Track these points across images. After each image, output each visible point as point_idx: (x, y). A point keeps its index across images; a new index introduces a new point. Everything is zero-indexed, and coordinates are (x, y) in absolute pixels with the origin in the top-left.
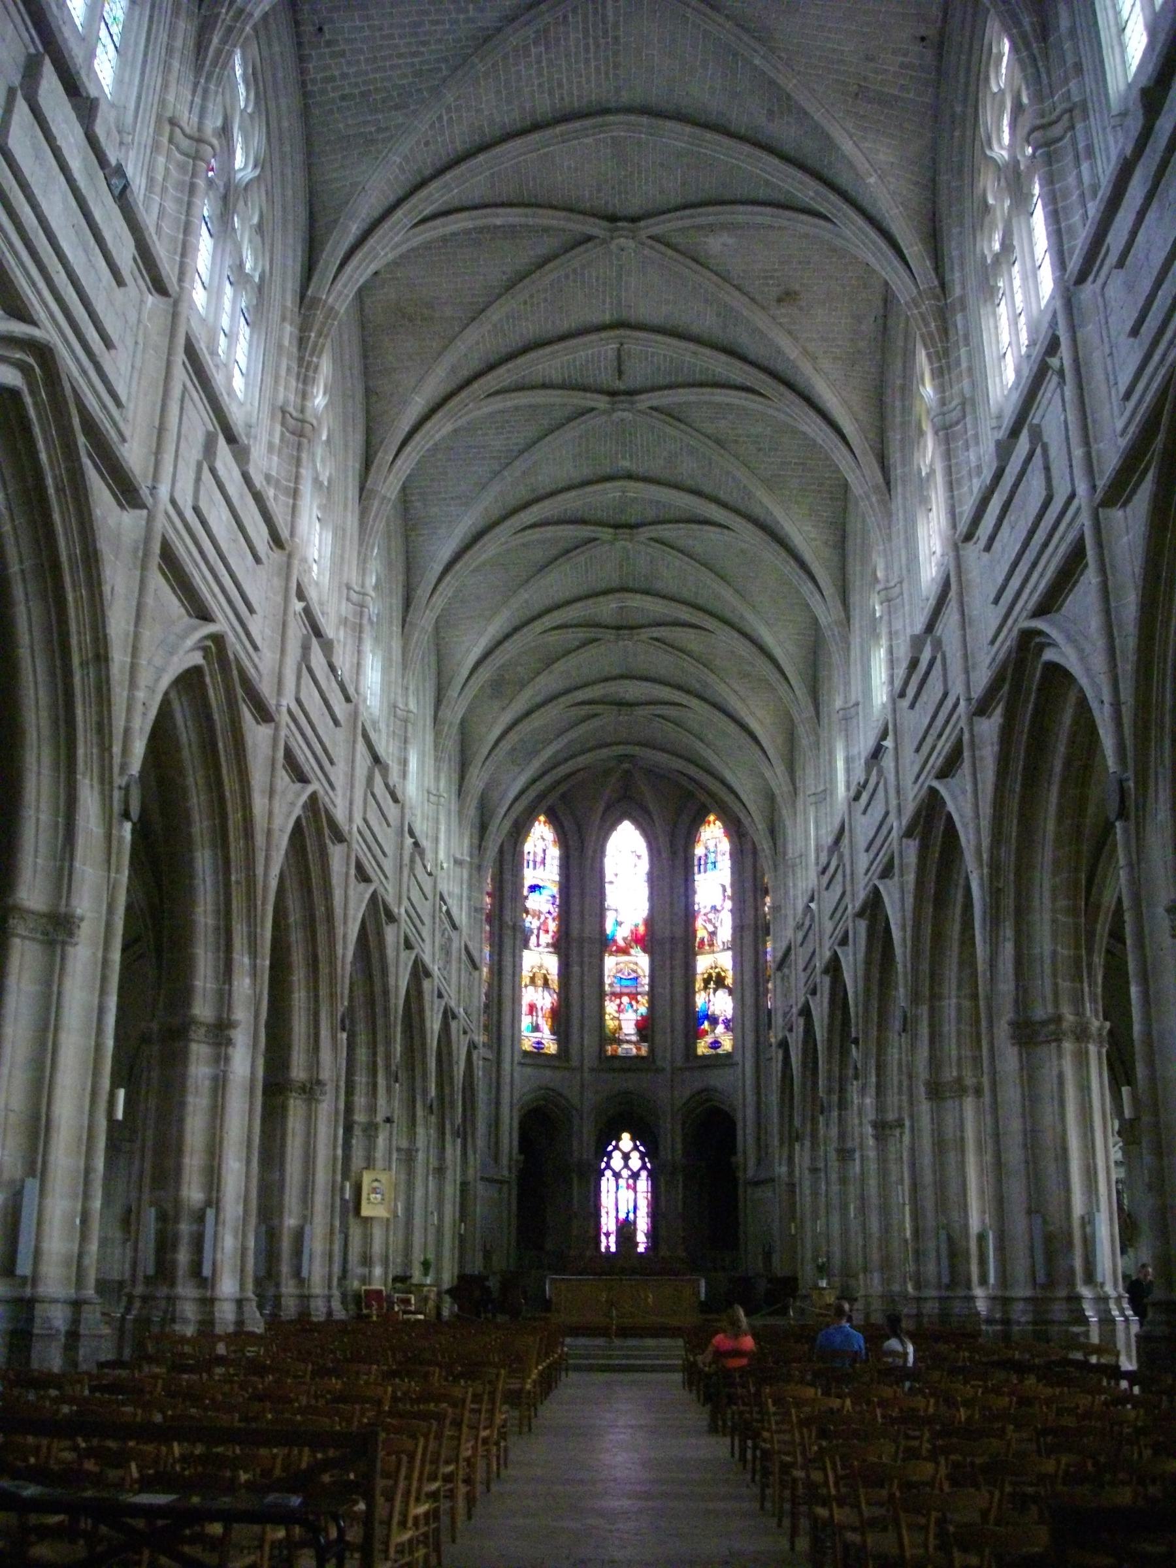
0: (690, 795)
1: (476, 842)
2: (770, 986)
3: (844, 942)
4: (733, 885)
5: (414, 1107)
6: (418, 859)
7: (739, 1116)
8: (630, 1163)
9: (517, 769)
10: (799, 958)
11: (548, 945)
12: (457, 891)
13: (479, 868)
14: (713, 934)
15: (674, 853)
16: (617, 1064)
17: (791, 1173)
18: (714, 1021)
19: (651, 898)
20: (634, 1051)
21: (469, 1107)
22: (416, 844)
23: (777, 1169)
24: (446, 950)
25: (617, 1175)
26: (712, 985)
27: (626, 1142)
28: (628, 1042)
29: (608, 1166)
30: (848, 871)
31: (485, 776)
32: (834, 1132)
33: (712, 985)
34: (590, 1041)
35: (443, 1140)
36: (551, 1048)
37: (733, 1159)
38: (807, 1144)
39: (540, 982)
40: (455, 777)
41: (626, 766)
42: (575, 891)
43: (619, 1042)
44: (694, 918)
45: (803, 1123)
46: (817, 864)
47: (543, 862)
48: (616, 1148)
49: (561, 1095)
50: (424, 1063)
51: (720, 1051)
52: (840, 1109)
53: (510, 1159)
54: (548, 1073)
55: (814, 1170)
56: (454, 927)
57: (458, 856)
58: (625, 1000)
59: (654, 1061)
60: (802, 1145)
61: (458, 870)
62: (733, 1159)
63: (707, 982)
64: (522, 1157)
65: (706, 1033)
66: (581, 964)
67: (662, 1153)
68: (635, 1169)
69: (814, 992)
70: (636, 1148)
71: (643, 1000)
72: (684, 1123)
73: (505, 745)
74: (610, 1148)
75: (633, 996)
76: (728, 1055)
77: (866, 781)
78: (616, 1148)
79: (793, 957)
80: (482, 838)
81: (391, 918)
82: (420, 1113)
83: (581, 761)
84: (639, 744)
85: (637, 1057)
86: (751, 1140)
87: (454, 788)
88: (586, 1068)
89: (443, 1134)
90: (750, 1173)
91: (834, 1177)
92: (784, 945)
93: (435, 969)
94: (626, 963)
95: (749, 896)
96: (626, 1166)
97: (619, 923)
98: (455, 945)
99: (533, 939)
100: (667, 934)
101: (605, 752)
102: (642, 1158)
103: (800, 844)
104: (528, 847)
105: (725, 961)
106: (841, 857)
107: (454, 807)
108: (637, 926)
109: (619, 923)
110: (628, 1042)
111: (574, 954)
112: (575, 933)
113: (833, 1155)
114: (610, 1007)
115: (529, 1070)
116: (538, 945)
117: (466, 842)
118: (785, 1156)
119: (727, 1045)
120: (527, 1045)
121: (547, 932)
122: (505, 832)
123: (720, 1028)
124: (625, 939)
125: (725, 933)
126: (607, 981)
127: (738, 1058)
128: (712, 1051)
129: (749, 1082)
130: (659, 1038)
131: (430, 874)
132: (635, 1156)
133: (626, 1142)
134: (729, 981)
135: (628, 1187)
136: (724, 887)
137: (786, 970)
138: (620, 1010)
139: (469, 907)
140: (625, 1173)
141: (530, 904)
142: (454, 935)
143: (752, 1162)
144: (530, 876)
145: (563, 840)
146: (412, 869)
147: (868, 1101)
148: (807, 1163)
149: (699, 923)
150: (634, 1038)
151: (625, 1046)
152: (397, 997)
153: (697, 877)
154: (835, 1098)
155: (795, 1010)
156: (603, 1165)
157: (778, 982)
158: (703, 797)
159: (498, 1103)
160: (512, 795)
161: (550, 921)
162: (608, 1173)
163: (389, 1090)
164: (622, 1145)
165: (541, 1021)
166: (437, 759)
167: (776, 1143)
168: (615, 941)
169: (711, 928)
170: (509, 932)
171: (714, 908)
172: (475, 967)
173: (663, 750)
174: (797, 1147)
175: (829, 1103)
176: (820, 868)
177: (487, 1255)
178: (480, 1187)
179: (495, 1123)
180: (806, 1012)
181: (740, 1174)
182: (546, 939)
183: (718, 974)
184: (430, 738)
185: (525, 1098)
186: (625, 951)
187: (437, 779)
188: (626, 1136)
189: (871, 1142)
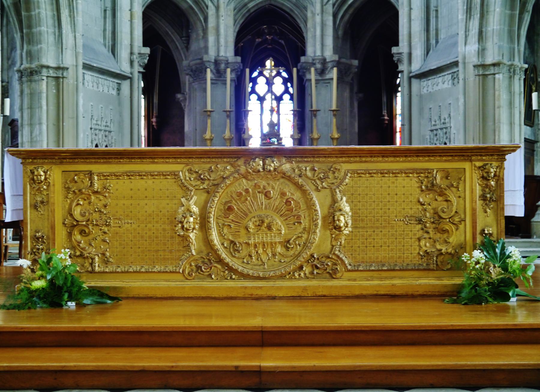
8: (274, 87)
17: (482, 52)
23: (461, 48)
25: (261, 99)
29: (253, 91)
53: (132, 53)
62: (394, 50)
64: (147, 50)
67: (310, 50)
68: (278, 94)
72: (335, 16)
74: (255, 74)
78: (261, 74)
86: (417, 26)
96: (270, 91)
132: (278, 81)
135: (272, 111)
140: (269, 97)
162: (254, 97)
164: (266, 73)
167: (461, 16)
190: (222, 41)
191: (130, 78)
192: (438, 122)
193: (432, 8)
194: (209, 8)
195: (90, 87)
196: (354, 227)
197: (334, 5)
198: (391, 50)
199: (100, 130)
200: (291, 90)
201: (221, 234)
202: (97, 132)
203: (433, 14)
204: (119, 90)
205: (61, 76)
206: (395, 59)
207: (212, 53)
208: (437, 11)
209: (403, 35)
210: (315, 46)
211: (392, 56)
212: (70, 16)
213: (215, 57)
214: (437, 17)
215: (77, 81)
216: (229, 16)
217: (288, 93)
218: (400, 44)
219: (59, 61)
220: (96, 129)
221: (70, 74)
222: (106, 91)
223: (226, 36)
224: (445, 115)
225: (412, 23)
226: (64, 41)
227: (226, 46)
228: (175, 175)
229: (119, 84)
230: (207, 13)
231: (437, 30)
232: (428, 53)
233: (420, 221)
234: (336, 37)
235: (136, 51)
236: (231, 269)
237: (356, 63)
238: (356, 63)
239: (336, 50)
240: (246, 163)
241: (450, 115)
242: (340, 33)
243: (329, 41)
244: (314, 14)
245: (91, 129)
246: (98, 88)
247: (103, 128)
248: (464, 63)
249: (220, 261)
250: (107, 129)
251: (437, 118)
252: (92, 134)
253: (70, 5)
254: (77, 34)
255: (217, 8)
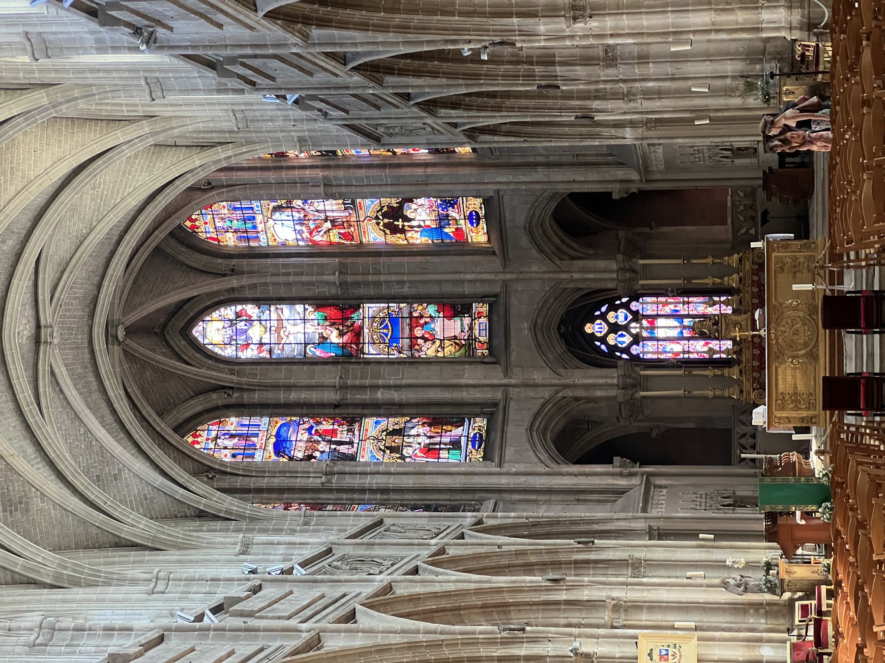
0: (158, 250)
1: (219, 524)
2: (399, 151)
3: (342, 59)
4: (273, 199)
5: (557, 603)
6: (236, 607)
7: (562, 188)
8: (621, 321)
9: (126, 474)
10: (365, 115)
11: (349, 431)
12: (282, 550)
13: (253, 519)
14: (333, 222)
15: (233, 272)
16: (499, 342)
17: (633, 124)
18: (443, 220)
19: (291, 300)
20: (483, 320)
21: (555, 529)
22: (217, 610)
23: (628, 142)
24: (356, 563)
25: (637, 339)
26: (400, 223)
27: (595, 328)
28: (471, 328)
29: (626, 350)
30: (249, 51)
31: (132, 516)
32: (580, 71)
33: (400, 223)
34: (470, 375)
35: (596, 562)
36: (481, 423)
37: (615, 196)
38: (596, 104)
39: (398, 440)
40: (133, 555)
41: (121, 334)
42: (282, 396)
43: (471, 339)
44: (315, 244)
45: (572, 109)
46: (242, 91)
47: (246, 437)
48: (603, 340)
49: (538, 413)
50: (499, 591)
51: (482, 213)
52: (553, 64)
53: (621, 475)
54: (510, 429)
55: (628, 96)
56: (329, 551)
57: (238, 548)
58: (418, 332)
59: (495, 296)
60: (598, 111)
61: (254, 549)
62: (615, 196)
63: (395, 230)
64: (617, 460)
65: (458, 230)
66: (377, 387)
67: (610, 285)
69: (407, 97)
70: (603, 317)
71: (418, 309)
72: (573, 258)
73: (94, 493)
74: (603, 347)
75: (414, 322)
76: (487, 202)
77: (128, 25)
78: (603, 340)
79: (363, 122)
80: (216, 518)
81: (315, 643)
82: (563, 596)
83: (115, 392)
84: (92, 315)
85: (490, 317)
86: (592, 175)
87: (147, 556)
88: (504, 381)
89: (587, 562)
90: (635, 176)
91: (638, 71)
92: (346, 132)
93: (381, 579)
94: (372, 332)
95: (284, 175)
96: (626, 328)
97: (323, 339)
98: (350, 551)
99: (343, 449)
100: (335, 278)
101: (103, 361)
102: (615, 309)
103: (218, 112)
104: (226, 457)
105: (370, 205)
106: (232, 60)
107: (173, 555)
108: (326, 319)
109: (323, 339)
110: (471, 328)
111: (359, 397)
112: (331, 396)
113: (611, 72)
114: (429, 351)
115: (509, 452)
116: (351, 443)
117: (219, 538)
118: (613, 131)
119: (475, 204)
120: (478, 455)
121: (334, 432)
122: (207, 488)
123: (453, 213)
124: (341, 334)
125: (333, 207)
126: (395, 355)
127: (490, 190)
128: (483, 224)
129: (523, 177)
130: (467, 289)
131: (256, 590)
132: (611, 317)
133: (595, 328)
134: (394, 202)
136: (276, 209)
137: (381, 130)
138: (430, 338)
139: (302, 531)
140: (635, 328)
141: (300, 455)
142: (338, 553)
143: (621, 173)
144: (265, 454)
145: (217, 412)
146: (251, 614)
147: (542, 28)
148: (620, 104)
149: (317, 238)
150: (467, 321)
151: (476, 332)
152: (418, 632)
153: (263, 242)
154: (538, 69)
155: (429, 121)
156: (625, 356)
157: (393, 140)
158: (160, 235)
159: (550, 491)
160: (160, 480)
161: (321, 428)
162: (635, 350)
163: (534, 640)
165: (446, 440)
166: (107, 584)
168: (344, 346)
169: (328, 225)
170: (335, 479)
171: (301, 222)
172: (380, 523)
173: (99, 286)
174: (599, 117)
175: (543, 77)
176: (247, 87)
177: (739, 503)
178: (653, 513)
179: (577, 495)
180: (431, 106)
181: (634, 189)
182: (342, 436)
183: (385, 215)
184: (78, 593)
185: (544, 456)
186: (358, 333)
187: (134, 582)
188: (589, 329)
189: (594, 24)
190: (601, 381)
191: (647, 477)
192: (696, 156)
193: (575, 160)
194: (565, 396)
195: (663, 510)
196: (798, 298)
197: (561, 259)
198: (616, 200)
199: (706, 502)
200: (624, 300)
201: (800, 350)
202: (708, 505)
203: (581, 159)
204: (661, 487)
205: (657, 532)
206: (625, 196)
207: (613, 393)
208: (577, 155)
209: (601, 188)
210: (606, 280)
211: (622, 198)
212: (598, 523)
213: (619, 389)
214: (584, 155)
215: (660, 518)
216: (573, 373)
217: (628, 303)
218: (609, 190)
219: (643, 534)
220: (706, 506)
221: (655, 524)
222: (665, 498)
223: (595, 377)
224: (691, 151)
225: (588, 179)
226: (624, 528)
227: (607, 377)
228: (776, 368)
229: (655, 486)
230: (571, 397)
231: (598, 155)
232: (622, 164)
233: (795, 273)
234: (596, 257)
235: (619, 470)
236: (814, 347)
237: (621, 234)
238: (621, 234)
239: (610, 256)
240: (773, 340)
241: (691, 147)
242: (591, 252)
243: (601, 264)
244: (571, 281)
245: (705, 510)
246: (662, 504)
247: (703, 500)
248: (643, 139)
249: (811, 350)
250: (704, 496)
251: (692, 157)
252: (711, 509)
253: (588, 523)
254: (615, 517)
255: (566, 386)
